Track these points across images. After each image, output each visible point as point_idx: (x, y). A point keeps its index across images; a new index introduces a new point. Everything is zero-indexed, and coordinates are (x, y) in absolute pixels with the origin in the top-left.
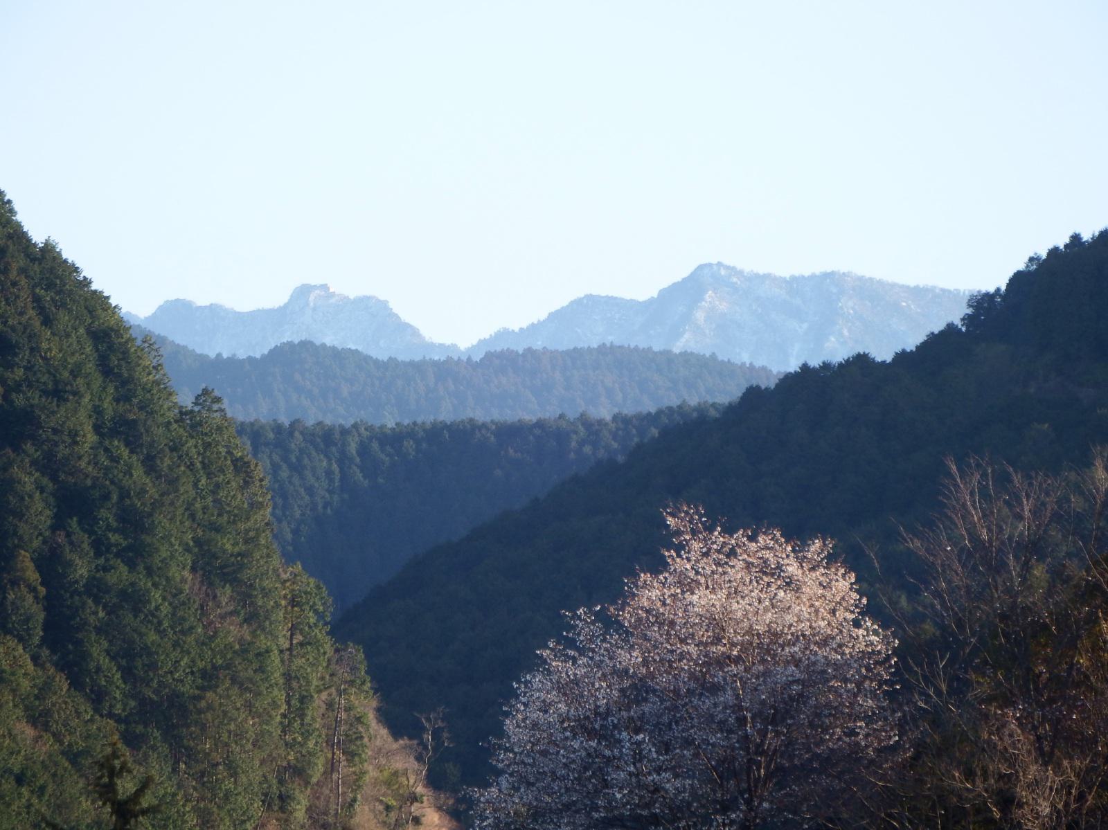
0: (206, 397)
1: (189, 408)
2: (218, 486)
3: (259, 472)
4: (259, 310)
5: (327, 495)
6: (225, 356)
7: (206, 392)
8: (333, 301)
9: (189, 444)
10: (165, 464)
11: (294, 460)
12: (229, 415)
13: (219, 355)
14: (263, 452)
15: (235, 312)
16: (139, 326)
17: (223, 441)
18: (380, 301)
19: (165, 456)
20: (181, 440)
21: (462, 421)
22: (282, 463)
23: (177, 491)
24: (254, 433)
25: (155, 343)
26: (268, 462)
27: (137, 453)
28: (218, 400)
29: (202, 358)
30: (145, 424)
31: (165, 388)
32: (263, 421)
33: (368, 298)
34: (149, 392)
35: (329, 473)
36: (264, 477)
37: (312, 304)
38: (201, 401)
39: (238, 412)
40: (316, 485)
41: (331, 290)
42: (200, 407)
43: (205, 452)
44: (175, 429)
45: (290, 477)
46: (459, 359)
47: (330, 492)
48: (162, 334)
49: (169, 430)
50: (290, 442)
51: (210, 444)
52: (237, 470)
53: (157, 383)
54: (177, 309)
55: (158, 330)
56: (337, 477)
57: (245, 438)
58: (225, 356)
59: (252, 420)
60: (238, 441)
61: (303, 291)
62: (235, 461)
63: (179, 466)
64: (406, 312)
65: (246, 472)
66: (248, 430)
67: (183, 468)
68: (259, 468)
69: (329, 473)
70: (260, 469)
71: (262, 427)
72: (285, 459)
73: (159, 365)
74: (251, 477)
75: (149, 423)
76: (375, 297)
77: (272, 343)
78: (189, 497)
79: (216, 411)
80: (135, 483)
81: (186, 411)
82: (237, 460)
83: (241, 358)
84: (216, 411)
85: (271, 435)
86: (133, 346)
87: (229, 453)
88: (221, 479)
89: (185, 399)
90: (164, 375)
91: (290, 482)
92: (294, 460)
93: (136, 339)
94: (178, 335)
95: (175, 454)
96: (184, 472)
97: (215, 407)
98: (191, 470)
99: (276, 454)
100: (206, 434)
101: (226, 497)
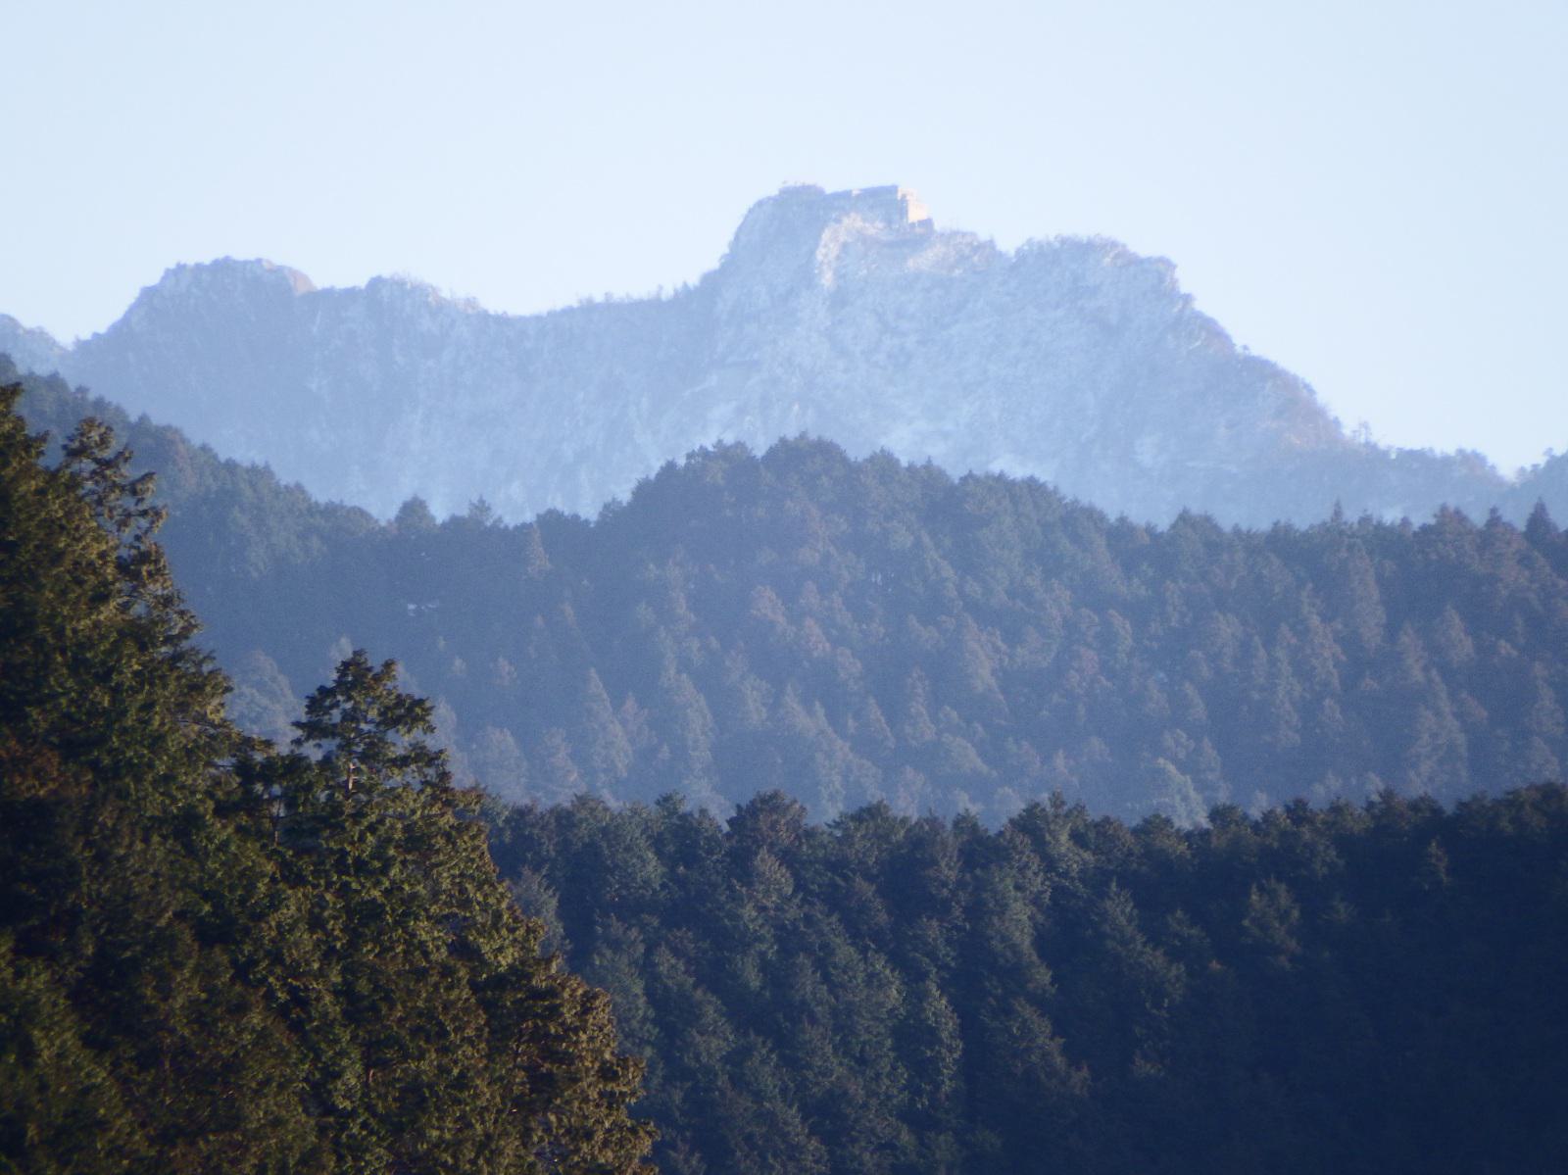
0: (359, 702)
1: (283, 748)
2: (415, 1098)
3: (597, 1039)
4: (588, 308)
5: (906, 1137)
6: (440, 511)
7: (355, 676)
8: (923, 261)
9: (289, 911)
10: (179, 1001)
11: (754, 980)
12: (461, 778)
13: (414, 509)
14: (616, 945)
15: (485, 316)
16: (54, 382)
17: (435, 895)
18: (1135, 261)
19: (179, 966)
20: (251, 888)
21: (1513, 801)
22: (699, 994)
23: (235, 1121)
24: (573, 856)
25: (123, 456)
26: (638, 988)
27: (52, 958)
28: (410, 712)
29: (339, 527)
30: (85, 829)
31: (177, 657)
32: (614, 804)
33: (1083, 250)
34: (104, 677)
35: (912, 1036)
36: (622, 1060)
37: (827, 280)
38: (336, 716)
39: (502, 764)
40: (856, 1089)
41: (915, 215)
42: (331, 744)
43: (353, 945)
44: (223, 846)
45: (737, 1058)
46: (1494, 520)
47: (921, 1123)
48: (159, 418)
49: (191, 850)
50: (734, 897)
51: (374, 911)
52: (499, 1036)
53: (140, 635)
54: (220, 305)
55: (136, 398)
56: (950, 1054)
57: (534, 883)
58: (440, 511)
59: (565, 800)
60: (504, 897)
61: (791, 217)
62: (491, 988)
63: (240, 1009)
64: (1254, 310)
65: (537, 1036)
66: (549, 848)
67: (256, 1019)
68: (602, 1015)
69: (912, 1036)
70: (606, 1020)
71: (611, 832)
72: (716, 976)
73: (144, 557)
74: (567, 1059)
75: (106, 817)
76: (1114, 244)
77: (651, 454)
78: (285, 1148)
79: (402, 762)
80: (43, 1088)
81: (269, 764)
82: (500, 982)
83: (510, 521)
84: (402, 762)
85: (652, 869)
86: (27, 472)
87: (463, 950)
88: (428, 1065)
89: (267, 708)
90: (167, 601)
91: (737, 1081)
92: (754, 980)
93: (43, 438)
94: (225, 422)
95: (221, 956)
96: (263, 1036)
97: (400, 741)
98: (296, 1027)
99: (676, 952)
100: (360, 866)
101: (455, 1146)
